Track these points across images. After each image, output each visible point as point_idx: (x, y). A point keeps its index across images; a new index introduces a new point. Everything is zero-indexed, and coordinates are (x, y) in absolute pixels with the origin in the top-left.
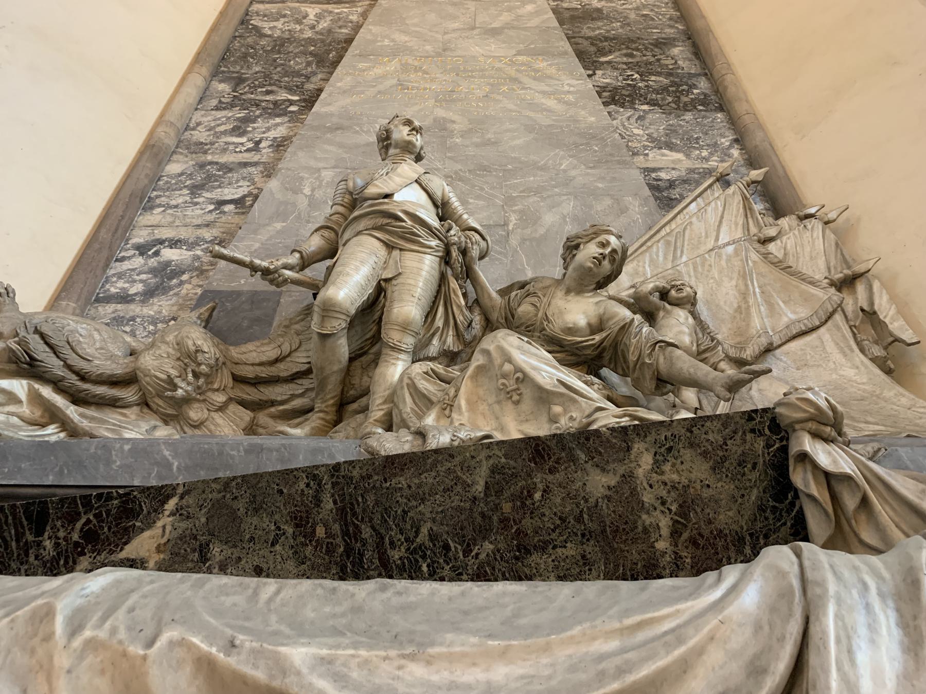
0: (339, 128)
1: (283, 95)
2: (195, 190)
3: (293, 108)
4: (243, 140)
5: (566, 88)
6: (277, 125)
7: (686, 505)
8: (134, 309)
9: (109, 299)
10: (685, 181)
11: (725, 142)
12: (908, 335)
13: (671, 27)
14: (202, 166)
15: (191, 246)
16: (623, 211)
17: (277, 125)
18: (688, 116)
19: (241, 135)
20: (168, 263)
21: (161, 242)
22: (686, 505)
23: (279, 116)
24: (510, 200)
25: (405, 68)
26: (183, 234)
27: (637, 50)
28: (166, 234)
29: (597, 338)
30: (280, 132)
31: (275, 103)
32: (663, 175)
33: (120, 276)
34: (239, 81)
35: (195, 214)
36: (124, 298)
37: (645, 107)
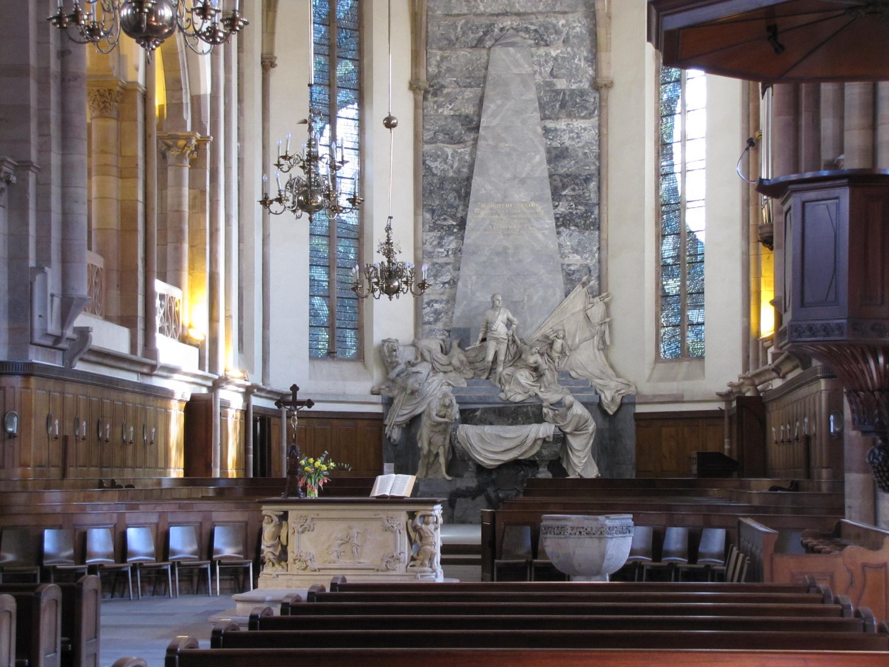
0: (474, 253)
1: (451, 222)
2: (435, 276)
3: (455, 230)
4: (442, 250)
5: (547, 226)
6: (452, 241)
7: (533, 412)
8: (433, 327)
9: (426, 323)
10: (578, 271)
11: (595, 249)
12: (608, 343)
13: (594, 164)
14: (434, 264)
15: (441, 302)
16: (555, 295)
17: (452, 241)
18: (587, 234)
19: (442, 247)
20: (436, 310)
21: (432, 301)
22: (533, 412)
23: (451, 235)
24: (525, 290)
25: (493, 212)
26: (437, 297)
27: (577, 184)
28: (433, 297)
29: (534, 365)
30: (453, 246)
31: (449, 227)
32: (572, 268)
33: (426, 314)
34: (433, 212)
35: (437, 287)
36: (429, 323)
37: (573, 228)
